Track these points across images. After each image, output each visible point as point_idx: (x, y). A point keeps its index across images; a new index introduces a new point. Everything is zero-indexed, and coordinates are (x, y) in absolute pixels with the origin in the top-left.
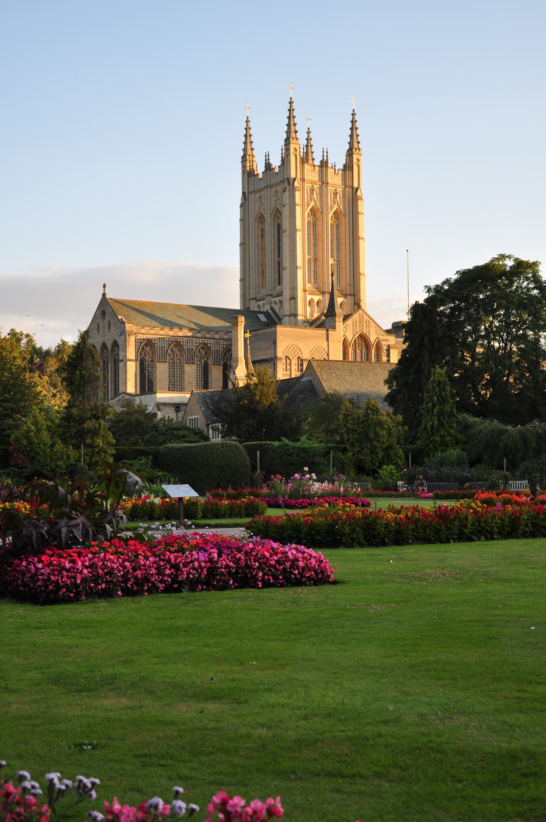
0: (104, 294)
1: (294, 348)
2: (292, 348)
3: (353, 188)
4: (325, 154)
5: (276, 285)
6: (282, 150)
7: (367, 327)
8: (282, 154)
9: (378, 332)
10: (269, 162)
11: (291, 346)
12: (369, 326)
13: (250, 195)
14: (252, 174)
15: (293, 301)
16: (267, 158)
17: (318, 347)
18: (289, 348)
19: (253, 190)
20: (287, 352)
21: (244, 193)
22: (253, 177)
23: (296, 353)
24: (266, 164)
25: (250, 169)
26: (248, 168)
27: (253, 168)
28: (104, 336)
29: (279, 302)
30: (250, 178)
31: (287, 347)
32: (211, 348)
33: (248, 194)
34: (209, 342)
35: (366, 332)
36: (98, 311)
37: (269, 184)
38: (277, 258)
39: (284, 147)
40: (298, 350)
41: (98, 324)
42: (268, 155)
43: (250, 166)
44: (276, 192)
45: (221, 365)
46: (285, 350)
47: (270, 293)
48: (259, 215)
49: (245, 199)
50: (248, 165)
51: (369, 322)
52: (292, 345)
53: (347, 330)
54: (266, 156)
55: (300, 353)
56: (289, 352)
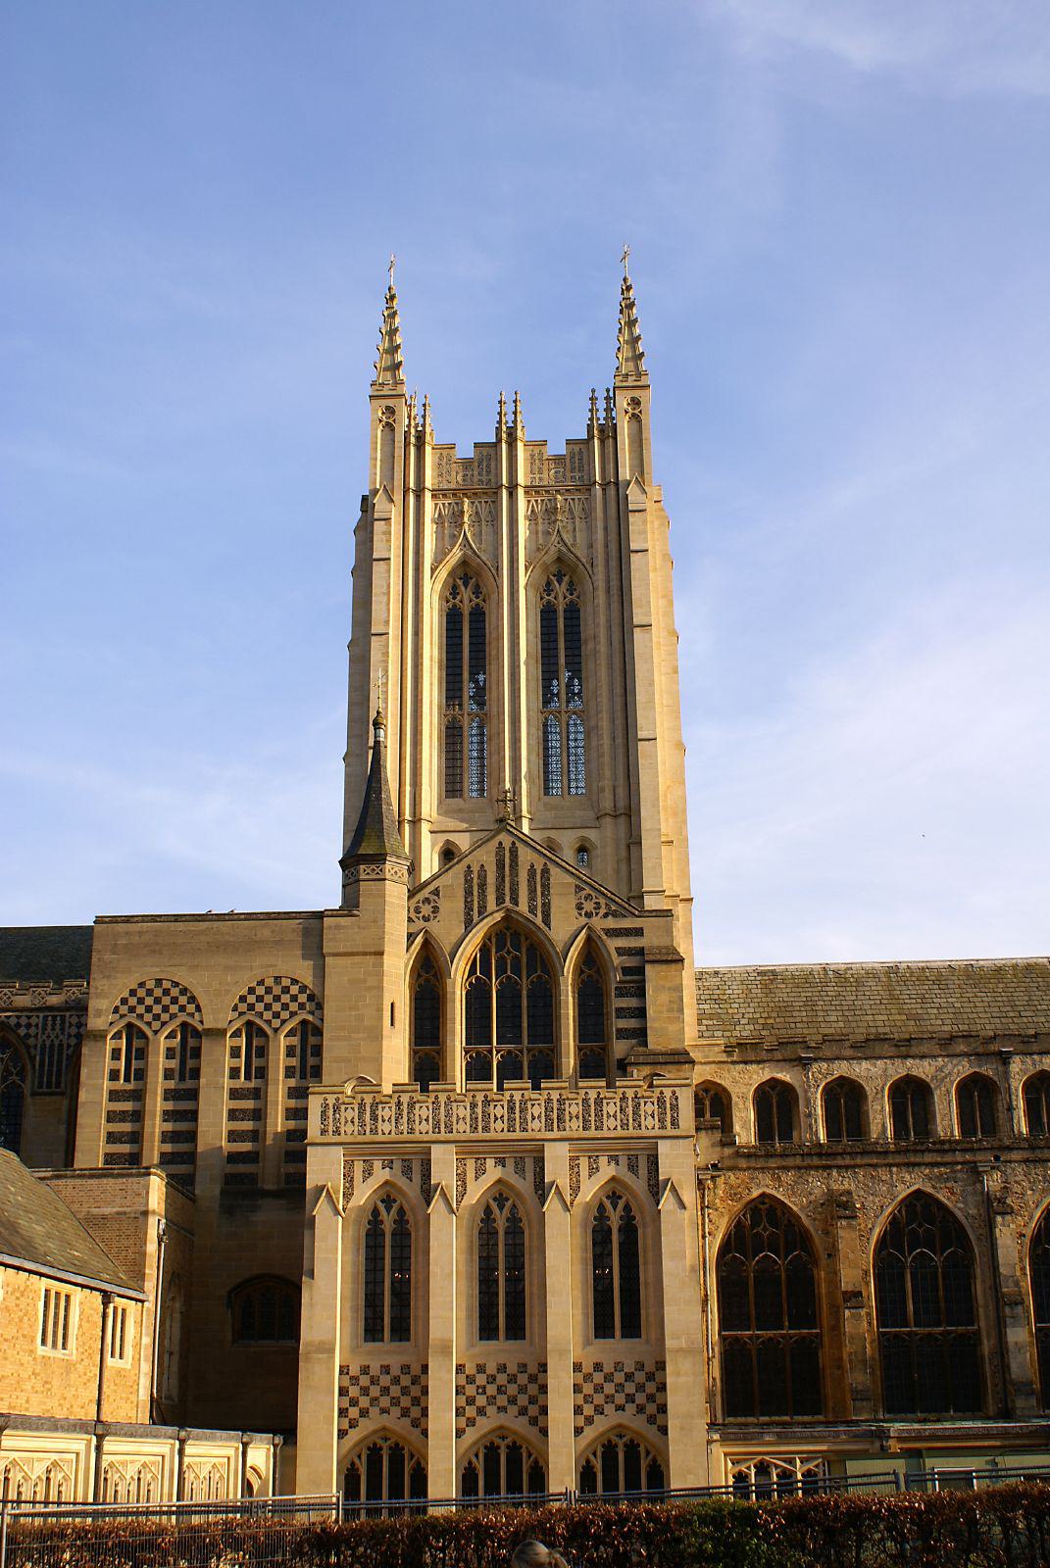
1: (166, 992)
2: (158, 992)
4: (508, 408)
7: (532, 891)
9: (588, 906)
11: (150, 985)
12: (546, 887)
17: (278, 979)
18: (141, 993)
20: (132, 1010)
23: (174, 1009)
31: (133, 993)
32: (31, 1041)
34: (23, 1021)
35: (533, 910)
40: (183, 1000)
45: (63, 1094)
46: (124, 1001)
51: (545, 871)
52: (159, 982)
53: (436, 910)
55: (191, 1008)
56: (141, 1009)
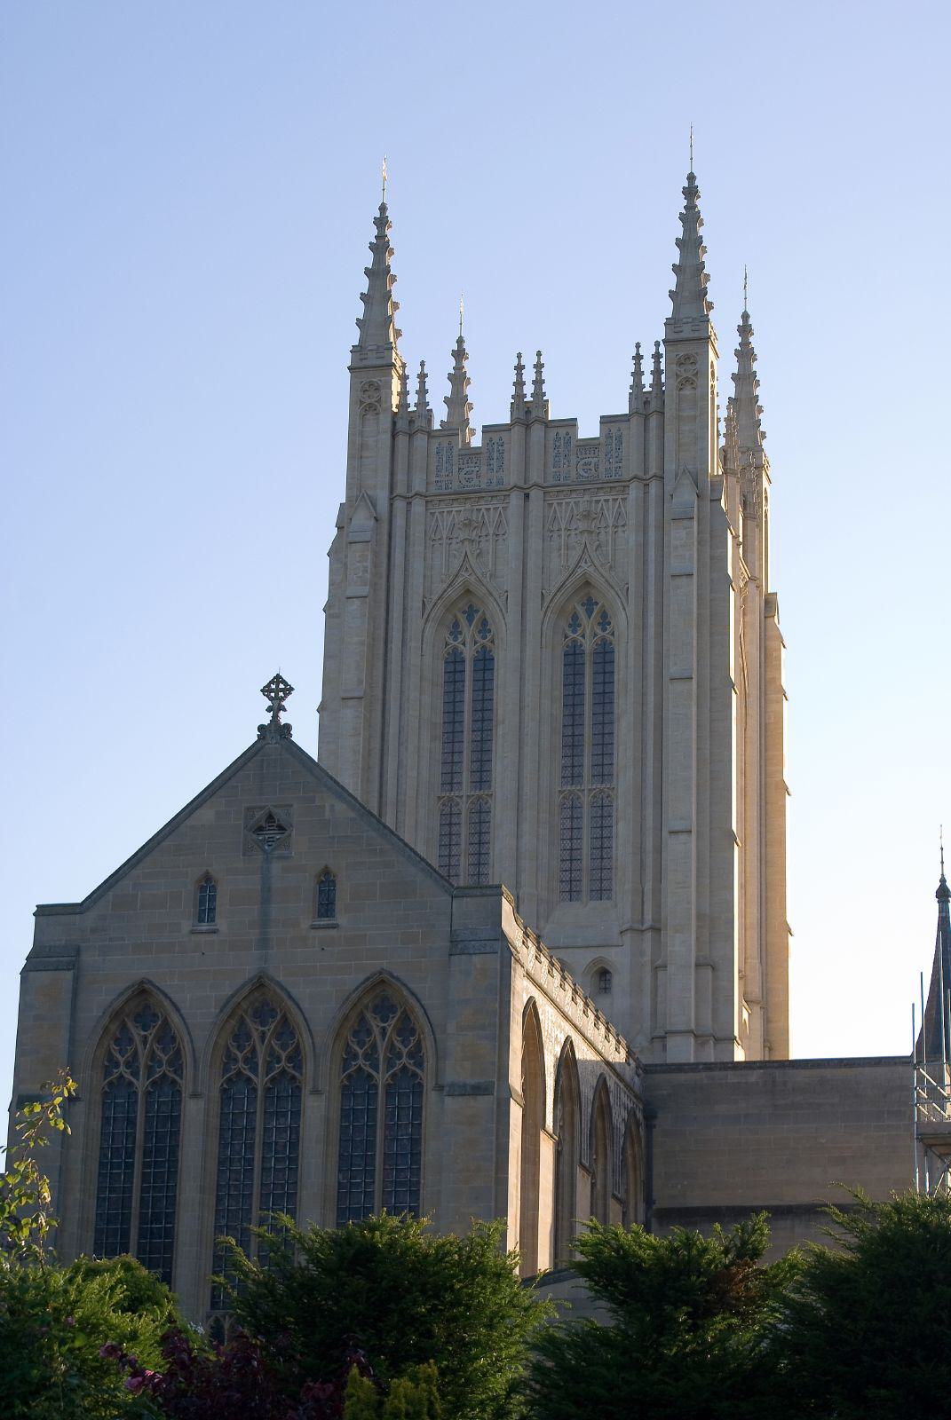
0: (275, 734)
3: (761, 592)
8: (638, 374)
10: (539, 393)
13: (400, 505)
14: (420, 423)
16: (529, 375)
19: (419, 486)
21: (357, 493)
22: (421, 440)
24: (519, 396)
25: (403, 405)
26: (395, 400)
27: (422, 403)
28: (264, 943)
30: (402, 441)
33: (391, 499)
36: (206, 815)
37: (535, 476)
39: (662, 350)
41: (207, 886)
42: (539, 367)
43: (404, 393)
48: (453, 593)
50: (396, 386)
54: (519, 368)
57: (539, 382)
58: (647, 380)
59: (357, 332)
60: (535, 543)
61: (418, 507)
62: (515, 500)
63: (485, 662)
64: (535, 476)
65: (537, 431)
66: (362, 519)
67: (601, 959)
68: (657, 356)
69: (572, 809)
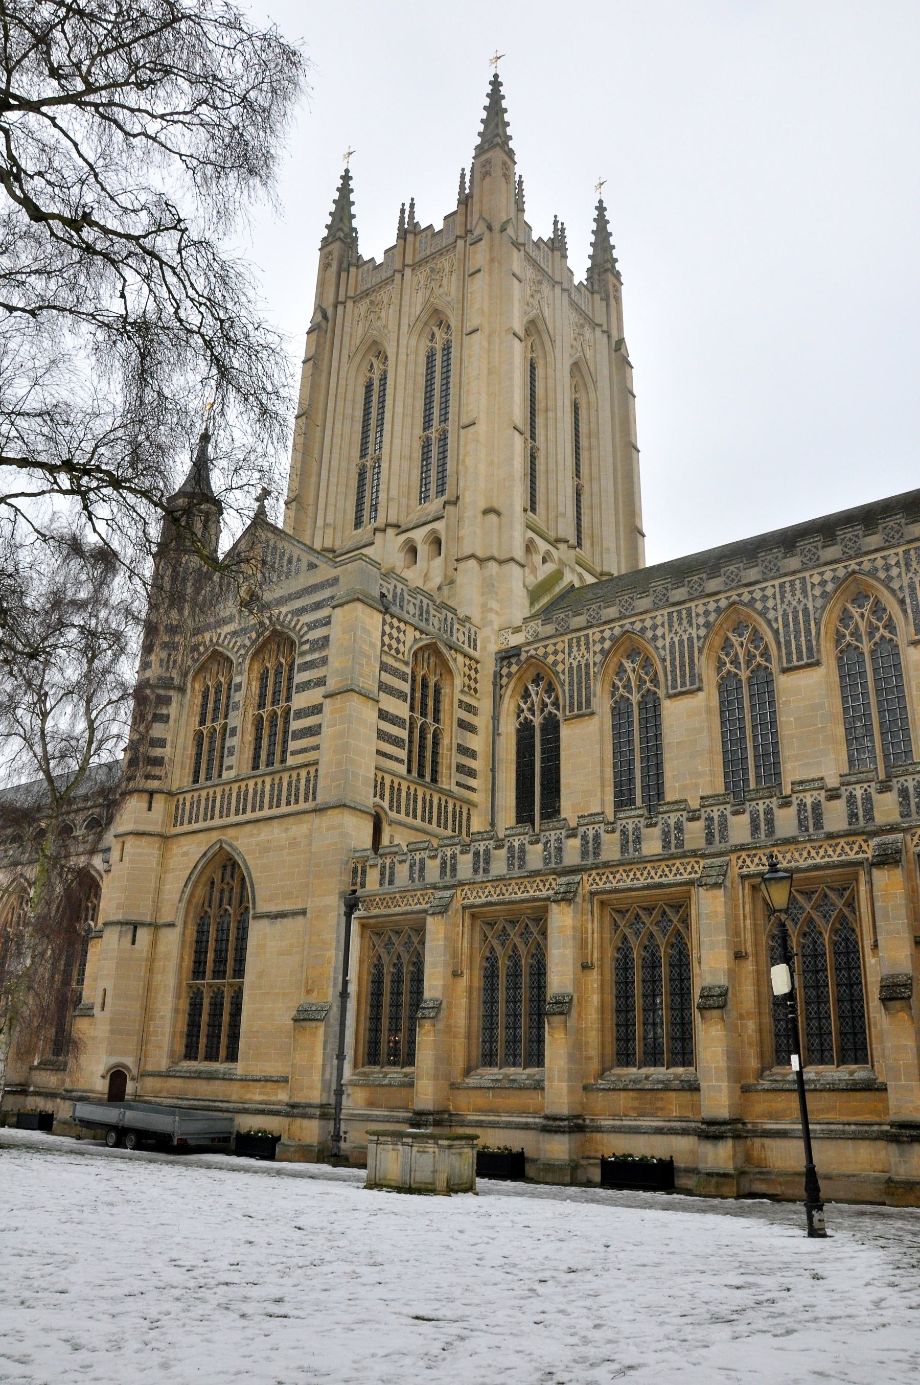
5: (414, 501)
6: (463, 176)
13: (340, 308)
15: (493, 517)
19: (351, 293)
21: (320, 309)
22: (353, 270)
29: (425, 541)
30: (344, 275)
38: (418, 431)
42: (412, 206)
44: (432, 270)
47: (392, 519)
49: (325, 317)
57: (412, 213)
58: (467, 185)
59: (326, 231)
60: (406, 298)
61: (350, 304)
62: (398, 276)
63: (384, 379)
64: (409, 261)
65: (410, 237)
66: (319, 318)
67: (434, 531)
68: (472, 170)
69: (426, 446)
